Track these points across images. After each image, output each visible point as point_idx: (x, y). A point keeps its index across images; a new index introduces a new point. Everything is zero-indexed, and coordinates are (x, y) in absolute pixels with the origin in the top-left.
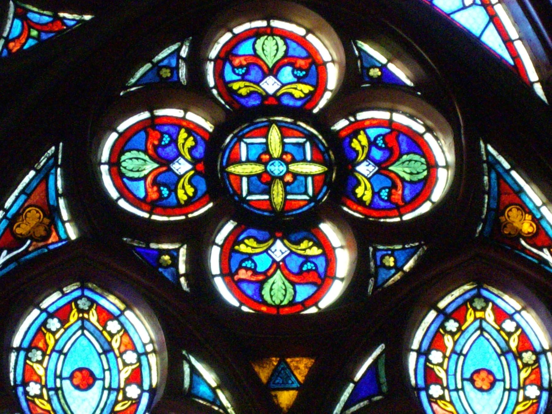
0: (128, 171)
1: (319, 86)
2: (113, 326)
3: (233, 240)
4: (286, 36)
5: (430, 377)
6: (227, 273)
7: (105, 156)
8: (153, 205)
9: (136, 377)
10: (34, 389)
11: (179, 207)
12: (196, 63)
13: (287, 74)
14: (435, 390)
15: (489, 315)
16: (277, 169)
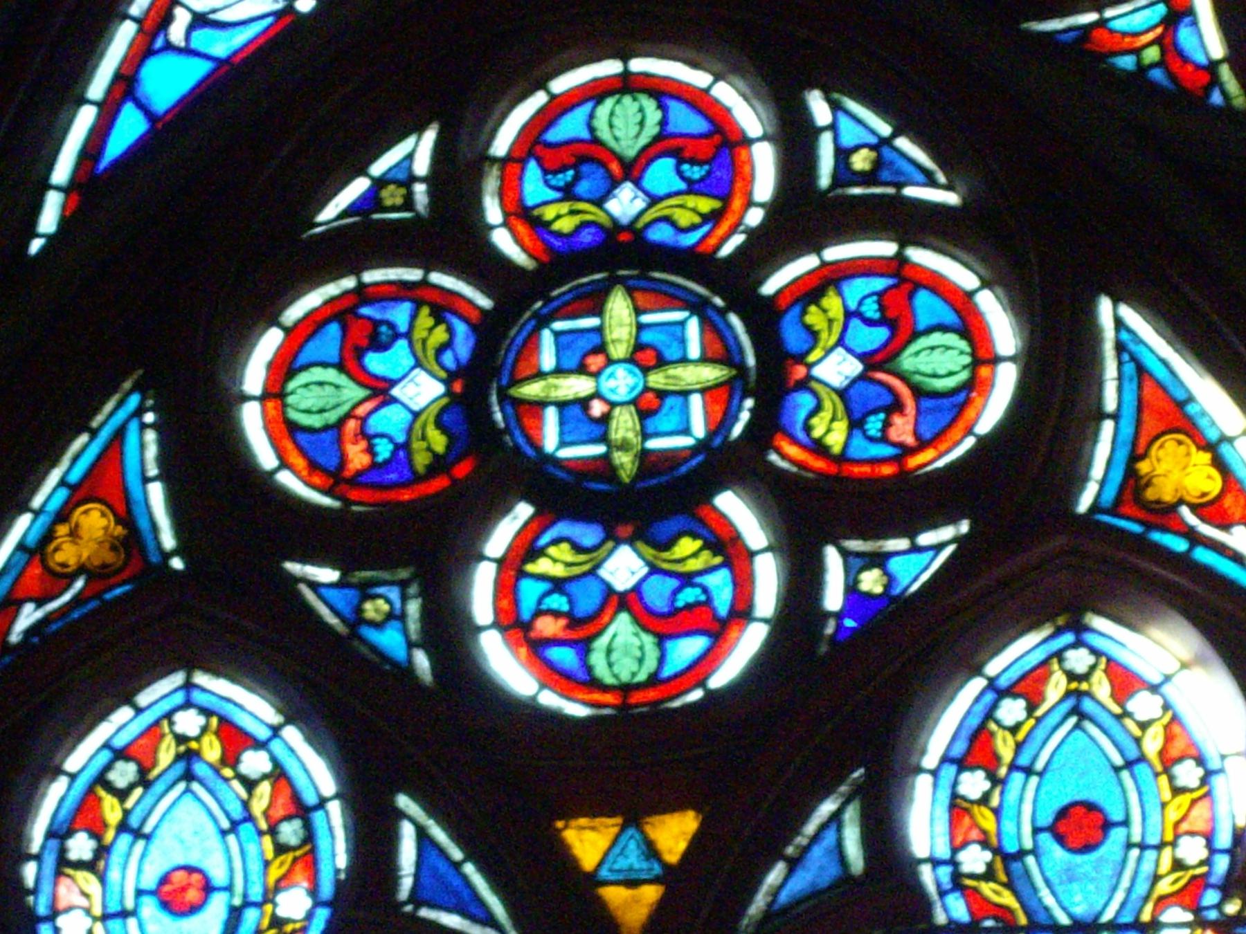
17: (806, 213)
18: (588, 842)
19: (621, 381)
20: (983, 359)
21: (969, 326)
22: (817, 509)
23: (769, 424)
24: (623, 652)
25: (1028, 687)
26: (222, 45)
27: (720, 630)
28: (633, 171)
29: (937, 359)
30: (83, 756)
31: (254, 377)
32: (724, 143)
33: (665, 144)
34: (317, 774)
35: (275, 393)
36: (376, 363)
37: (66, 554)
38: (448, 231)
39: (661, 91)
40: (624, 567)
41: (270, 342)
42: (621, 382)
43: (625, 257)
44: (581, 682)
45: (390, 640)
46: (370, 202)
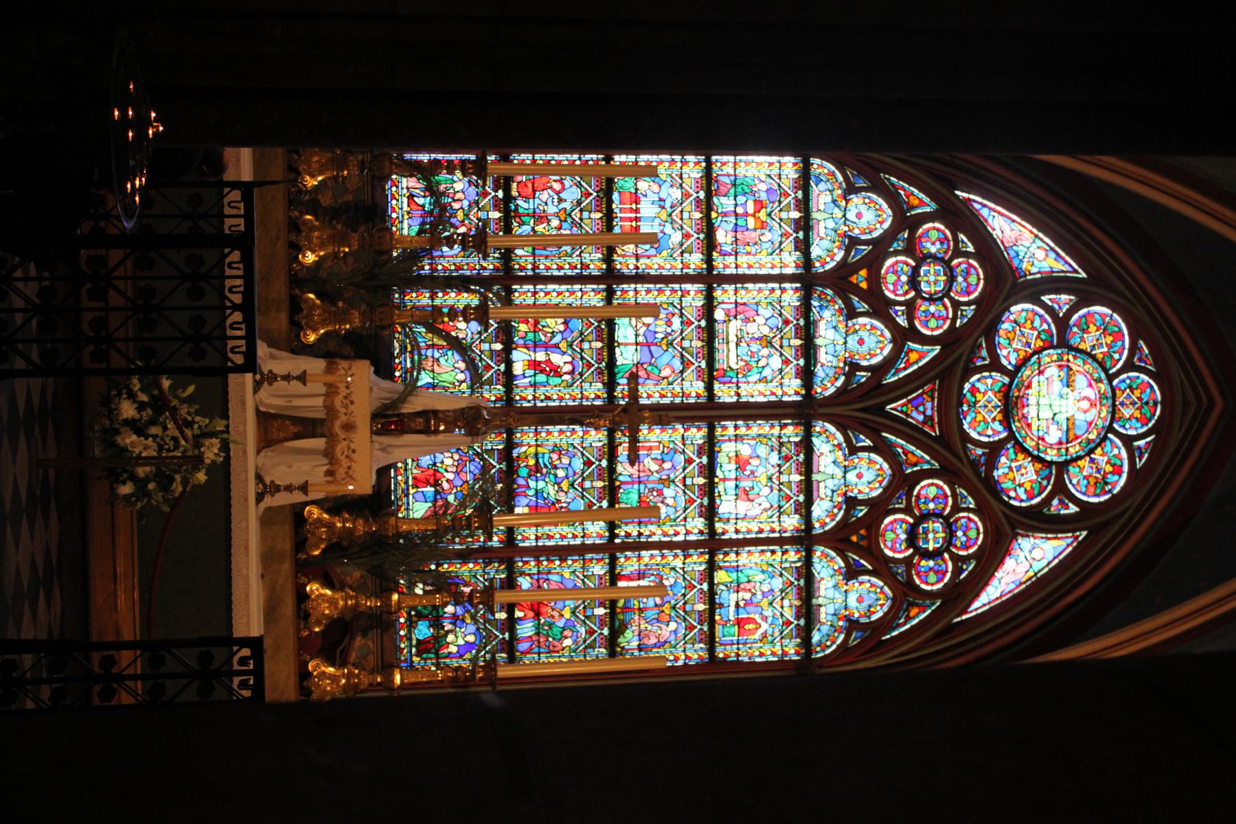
0: (929, 489)
1: (959, 549)
2: (877, 485)
3: (907, 522)
4: (977, 539)
5: (861, 583)
6: (895, 520)
7: (936, 481)
8: (918, 497)
9: (860, 492)
10: (856, 461)
11: (918, 506)
12: (968, 510)
13: (964, 539)
14: (857, 585)
15: (881, 602)
16: (931, 536)
17: (956, 305)
18: (863, 273)
19: (932, 280)
20: (932, 330)
21: (937, 328)
22: (910, 307)
23: (924, 299)
24: (891, 278)
25: (882, 335)
26: (990, 220)
27: (894, 292)
28: (965, 280)
29: (933, 323)
30: (881, 201)
31: (937, 225)
32: (969, 294)
33: (969, 285)
34: (875, 234)
35: (934, 228)
36: (938, 243)
37: (911, 198)
38: (958, 253)
39: (978, 284)
40: (904, 278)
41: (942, 227)
42: (932, 278)
43: (951, 279)
44: (887, 273)
45: (895, 245)
46: (963, 242)
